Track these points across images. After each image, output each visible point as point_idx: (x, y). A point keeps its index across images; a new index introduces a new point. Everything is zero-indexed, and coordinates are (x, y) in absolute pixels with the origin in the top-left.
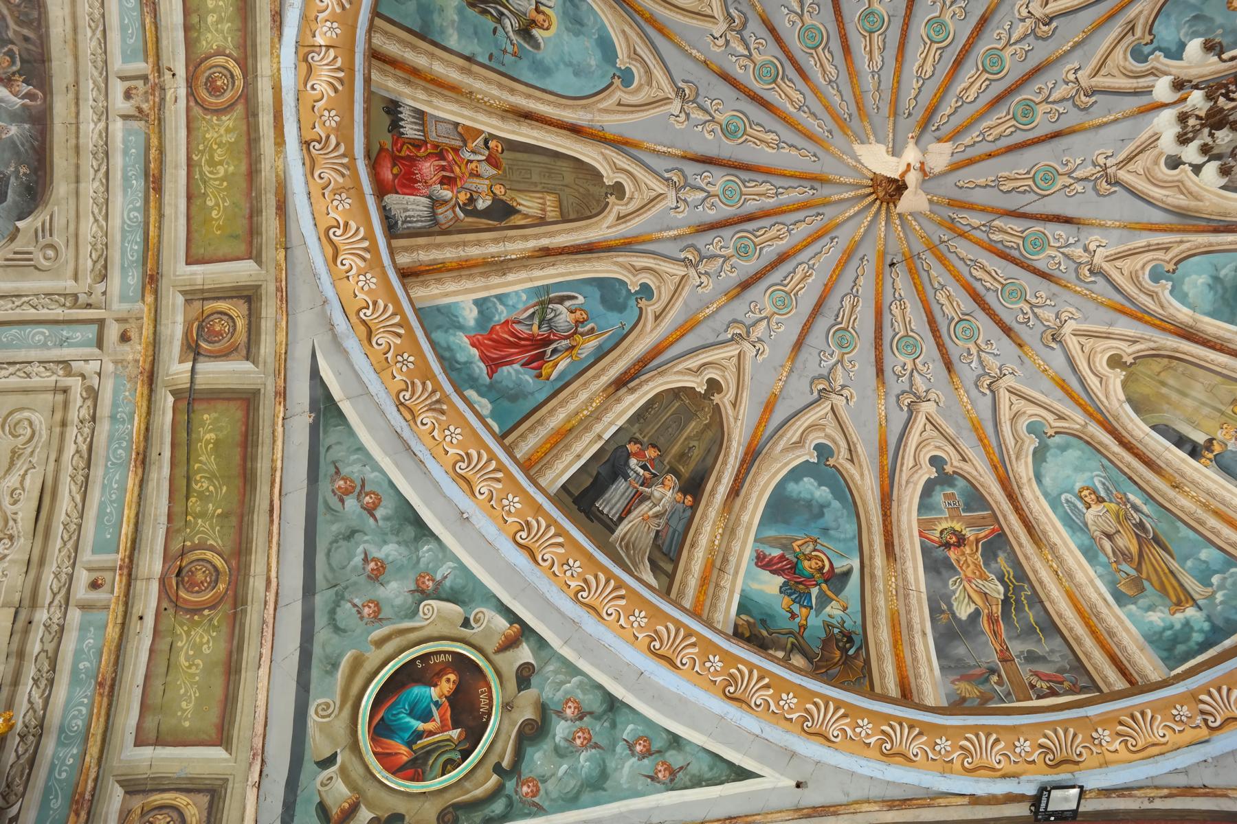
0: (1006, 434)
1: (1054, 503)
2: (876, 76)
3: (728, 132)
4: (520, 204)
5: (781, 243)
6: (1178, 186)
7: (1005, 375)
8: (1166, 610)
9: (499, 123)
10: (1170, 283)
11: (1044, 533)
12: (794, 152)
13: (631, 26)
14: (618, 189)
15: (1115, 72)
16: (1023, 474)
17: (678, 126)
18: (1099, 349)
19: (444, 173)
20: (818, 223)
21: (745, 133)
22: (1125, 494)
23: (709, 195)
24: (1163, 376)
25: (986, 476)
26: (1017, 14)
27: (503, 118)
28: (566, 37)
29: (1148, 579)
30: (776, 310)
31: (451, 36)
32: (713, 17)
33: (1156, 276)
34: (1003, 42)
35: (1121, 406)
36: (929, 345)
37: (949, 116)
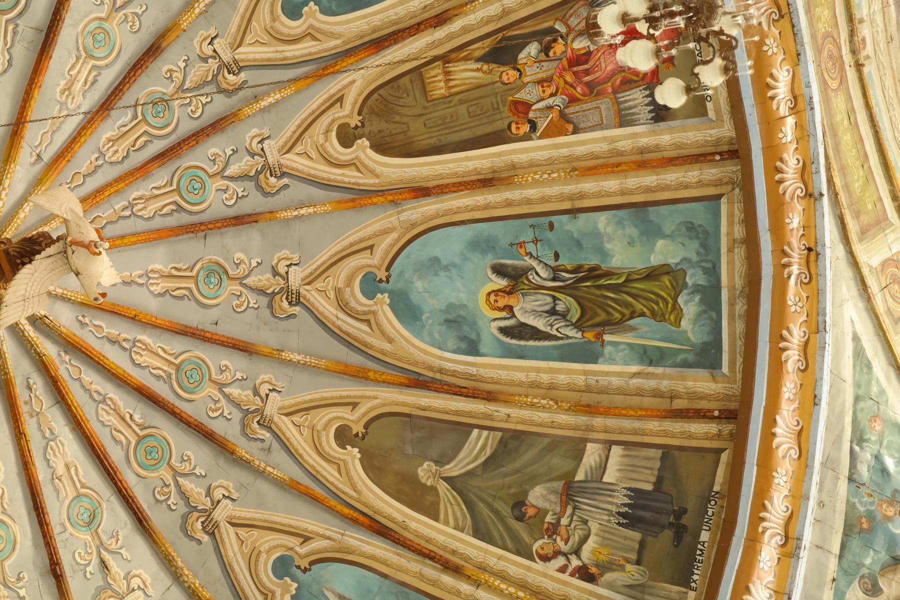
2: (48, 434)
3: (218, 272)
4: (478, 70)
5: (109, 134)
9: (516, 158)
13: (383, 352)
14: (347, 137)
17: (285, 253)
19: (586, 67)
21: (195, 278)
23: (220, 174)
27: (513, 167)
28: (463, 297)
30: (106, 25)
31: (607, 225)
32: (287, 415)
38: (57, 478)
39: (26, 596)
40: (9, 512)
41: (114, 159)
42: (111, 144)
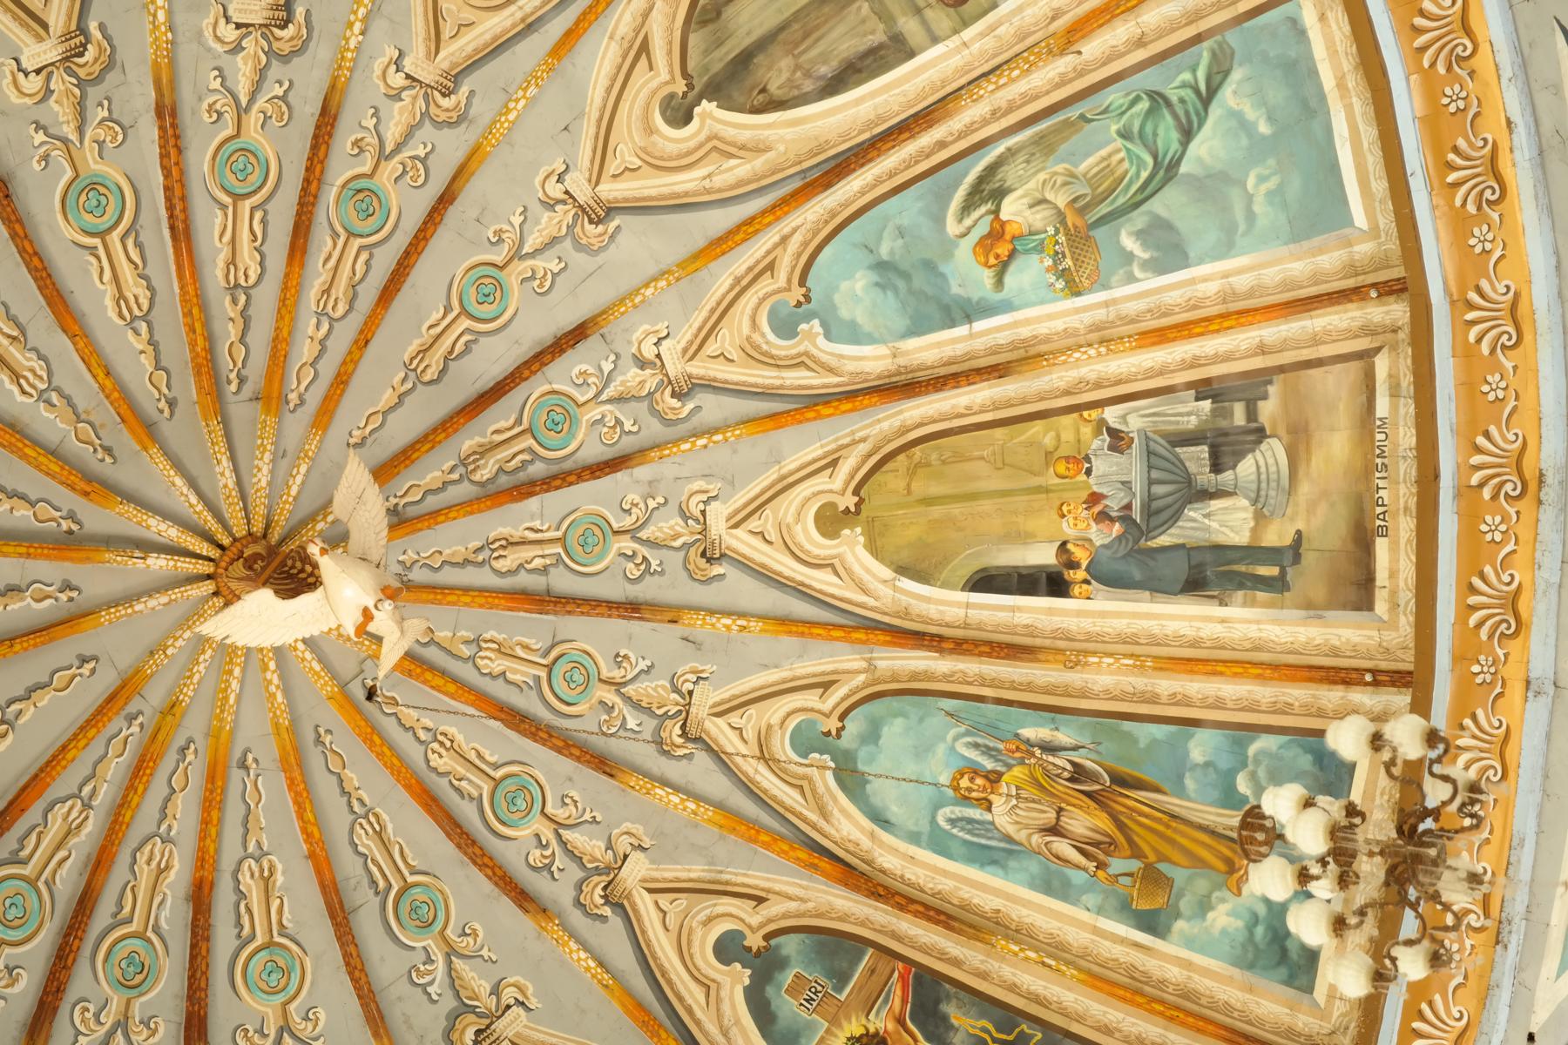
0: (775, 792)
1: (939, 843)
2: (54, 397)
5: (172, 874)
6: (715, 148)
7: (691, 693)
8: (1227, 894)
10: (816, 322)
11: (965, 907)
12: (45, 699)
15: (468, 15)
16: (856, 835)
18: (790, 519)
20: (196, 765)
22: (1017, 735)
24: (921, 487)
25: (810, 894)
26: (219, 48)
29: (1163, 858)
30: (280, 998)
33: (786, 328)
34: (230, 117)
35: (895, 589)
36: (544, 763)
37: (242, 340)
38: (14, 338)
39: (33, 133)
40: (86, 252)
41: (148, 848)
42: (162, 866)
